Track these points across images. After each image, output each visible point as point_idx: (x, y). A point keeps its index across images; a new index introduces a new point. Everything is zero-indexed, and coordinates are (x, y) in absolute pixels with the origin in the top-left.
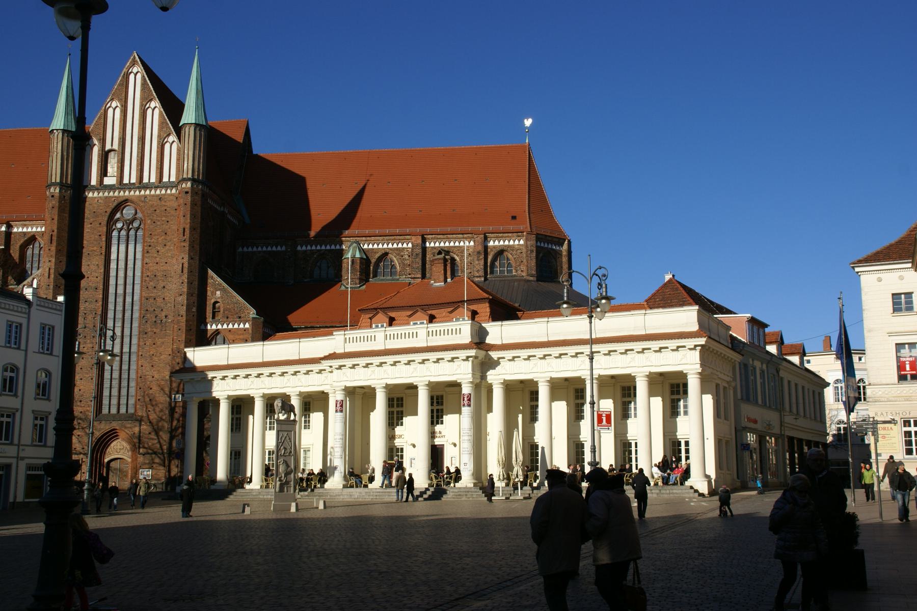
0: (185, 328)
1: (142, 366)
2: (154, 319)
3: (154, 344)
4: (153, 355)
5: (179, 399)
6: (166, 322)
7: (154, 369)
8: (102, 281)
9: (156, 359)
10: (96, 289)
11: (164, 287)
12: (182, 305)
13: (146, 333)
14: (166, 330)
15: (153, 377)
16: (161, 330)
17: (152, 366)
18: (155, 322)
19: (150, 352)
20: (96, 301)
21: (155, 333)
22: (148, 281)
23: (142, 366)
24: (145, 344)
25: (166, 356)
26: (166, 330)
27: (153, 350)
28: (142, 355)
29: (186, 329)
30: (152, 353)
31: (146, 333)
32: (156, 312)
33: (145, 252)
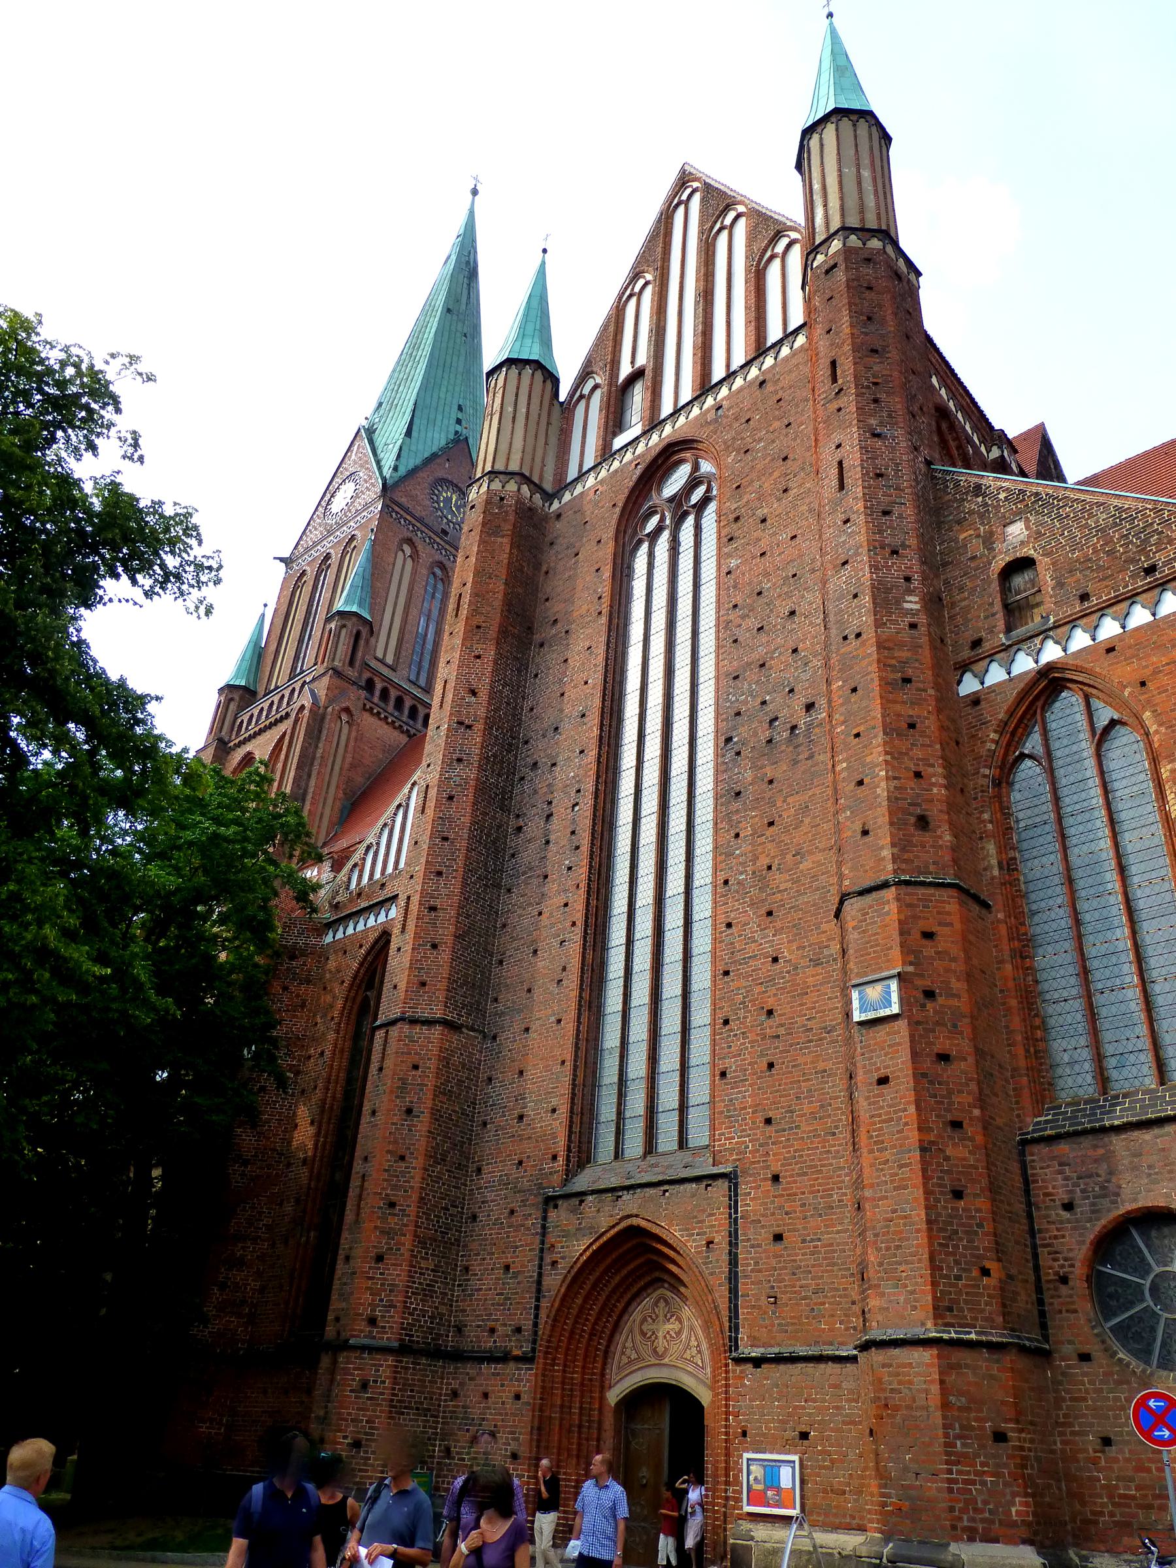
0: (875, 676)
1: (729, 925)
2: (764, 736)
3: (771, 824)
4: (769, 868)
5: (889, 1004)
6: (809, 726)
7: (778, 924)
8: (599, 688)
9: (778, 879)
10: (583, 716)
11: (793, 613)
12: (855, 596)
13: (738, 794)
14: (811, 757)
15: (775, 960)
16: (795, 762)
17: (770, 913)
18: (770, 741)
19: (755, 859)
20: (582, 752)
21: (771, 782)
22: (739, 621)
23: (729, 925)
24: (737, 835)
25: (820, 857)
26: (811, 757)
27: (769, 846)
28: (726, 882)
29: (881, 679)
30: (764, 861)
31: (738, 794)
32: (770, 707)
33: (727, 540)
